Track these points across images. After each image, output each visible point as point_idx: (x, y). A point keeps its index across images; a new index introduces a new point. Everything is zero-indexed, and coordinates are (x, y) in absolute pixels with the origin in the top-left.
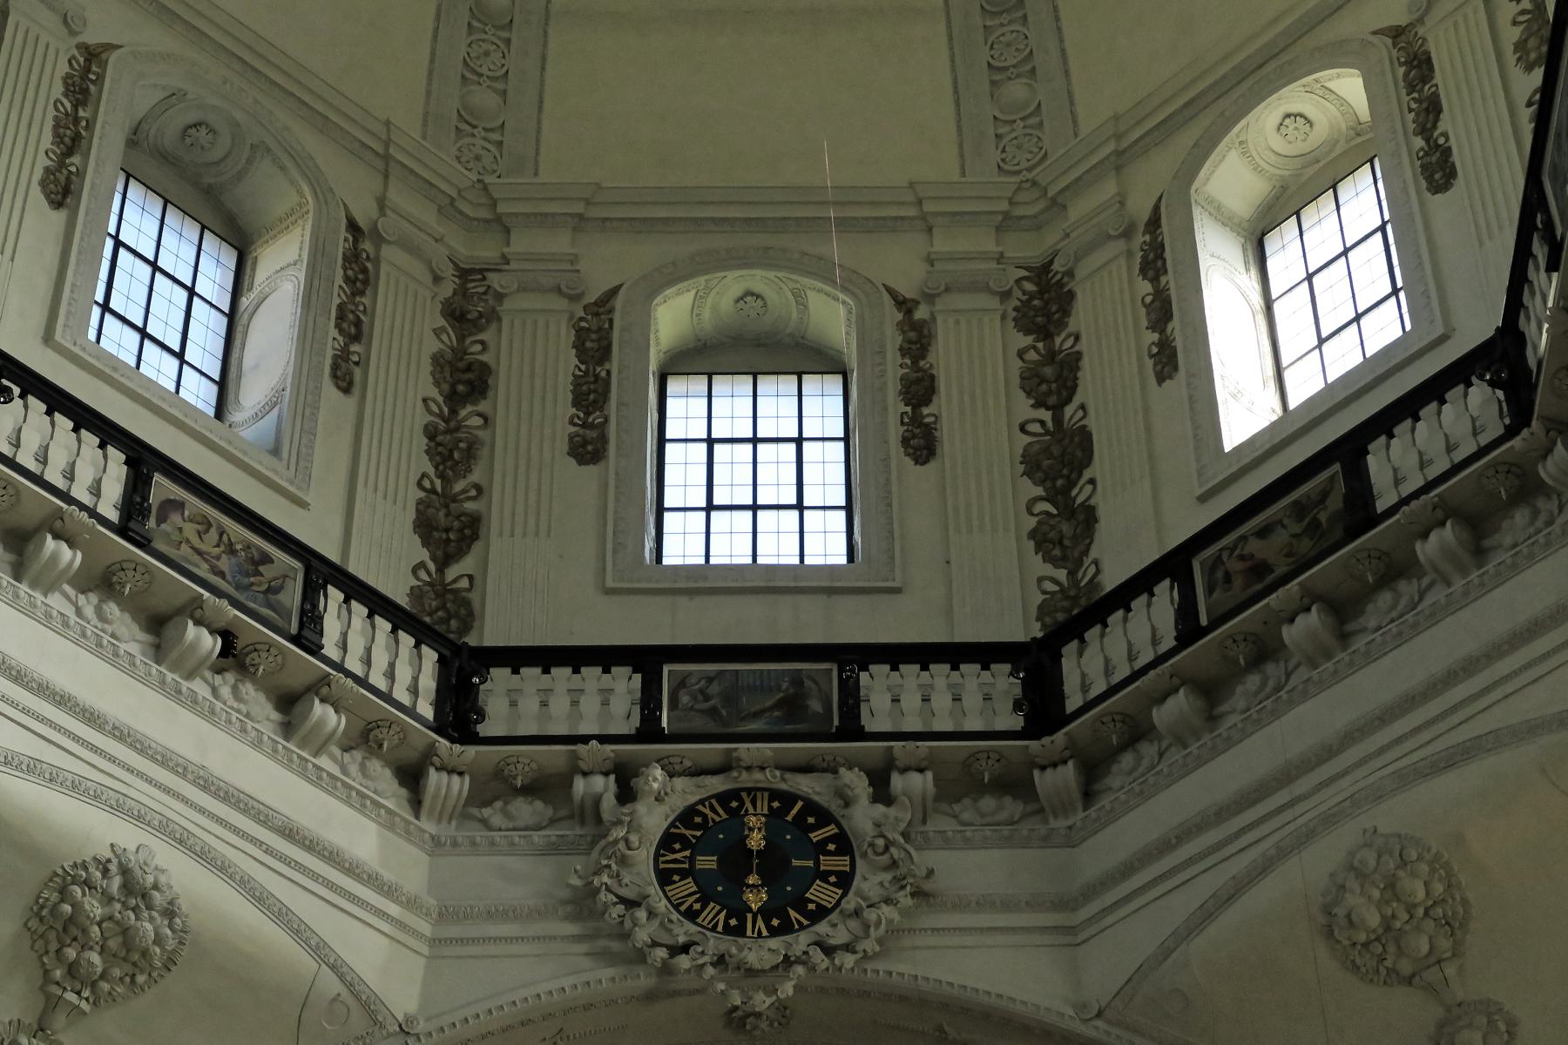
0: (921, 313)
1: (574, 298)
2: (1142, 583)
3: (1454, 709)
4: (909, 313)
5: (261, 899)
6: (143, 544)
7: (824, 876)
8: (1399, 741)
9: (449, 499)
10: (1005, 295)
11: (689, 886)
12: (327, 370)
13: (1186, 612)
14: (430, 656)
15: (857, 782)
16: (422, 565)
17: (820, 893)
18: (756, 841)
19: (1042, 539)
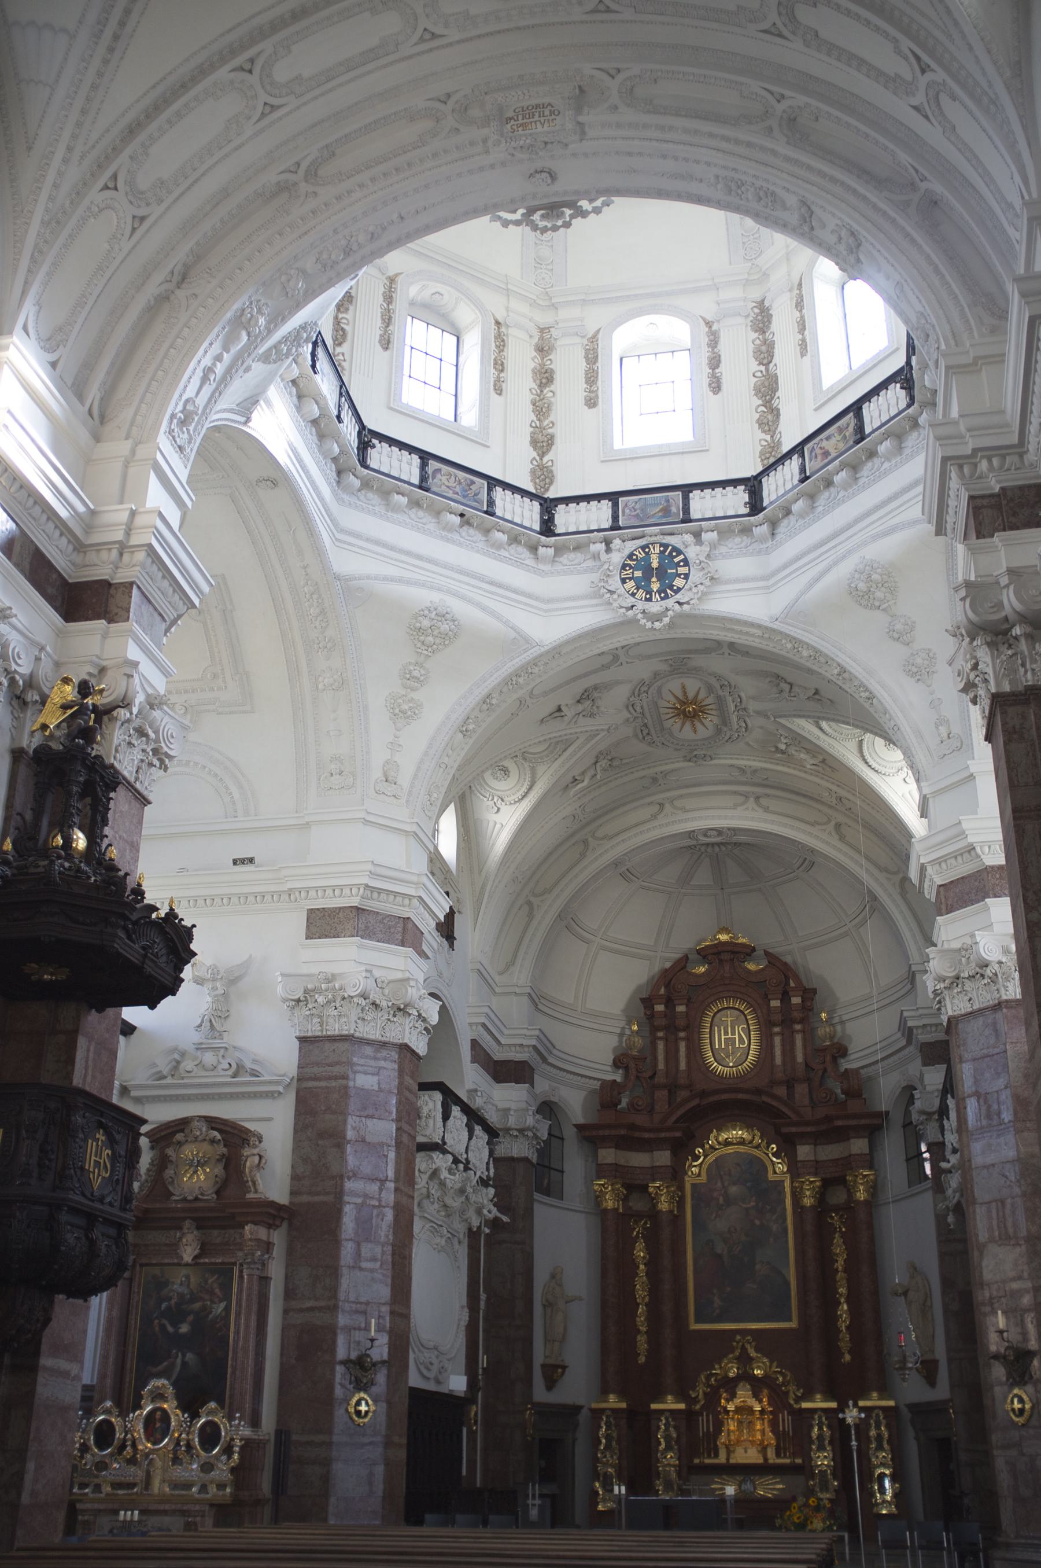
0: (714, 328)
1: (583, 337)
2: (789, 455)
3: (890, 512)
4: (710, 327)
5: (484, 609)
6: (427, 490)
7: (679, 575)
8: (873, 523)
9: (542, 429)
10: (747, 316)
11: (632, 583)
12: (492, 387)
13: (803, 469)
14: (536, 505)
15: (689, 538)
16: (534, 459)
17: (678, 582)
18: (655, 564)
19: (762, 424)
